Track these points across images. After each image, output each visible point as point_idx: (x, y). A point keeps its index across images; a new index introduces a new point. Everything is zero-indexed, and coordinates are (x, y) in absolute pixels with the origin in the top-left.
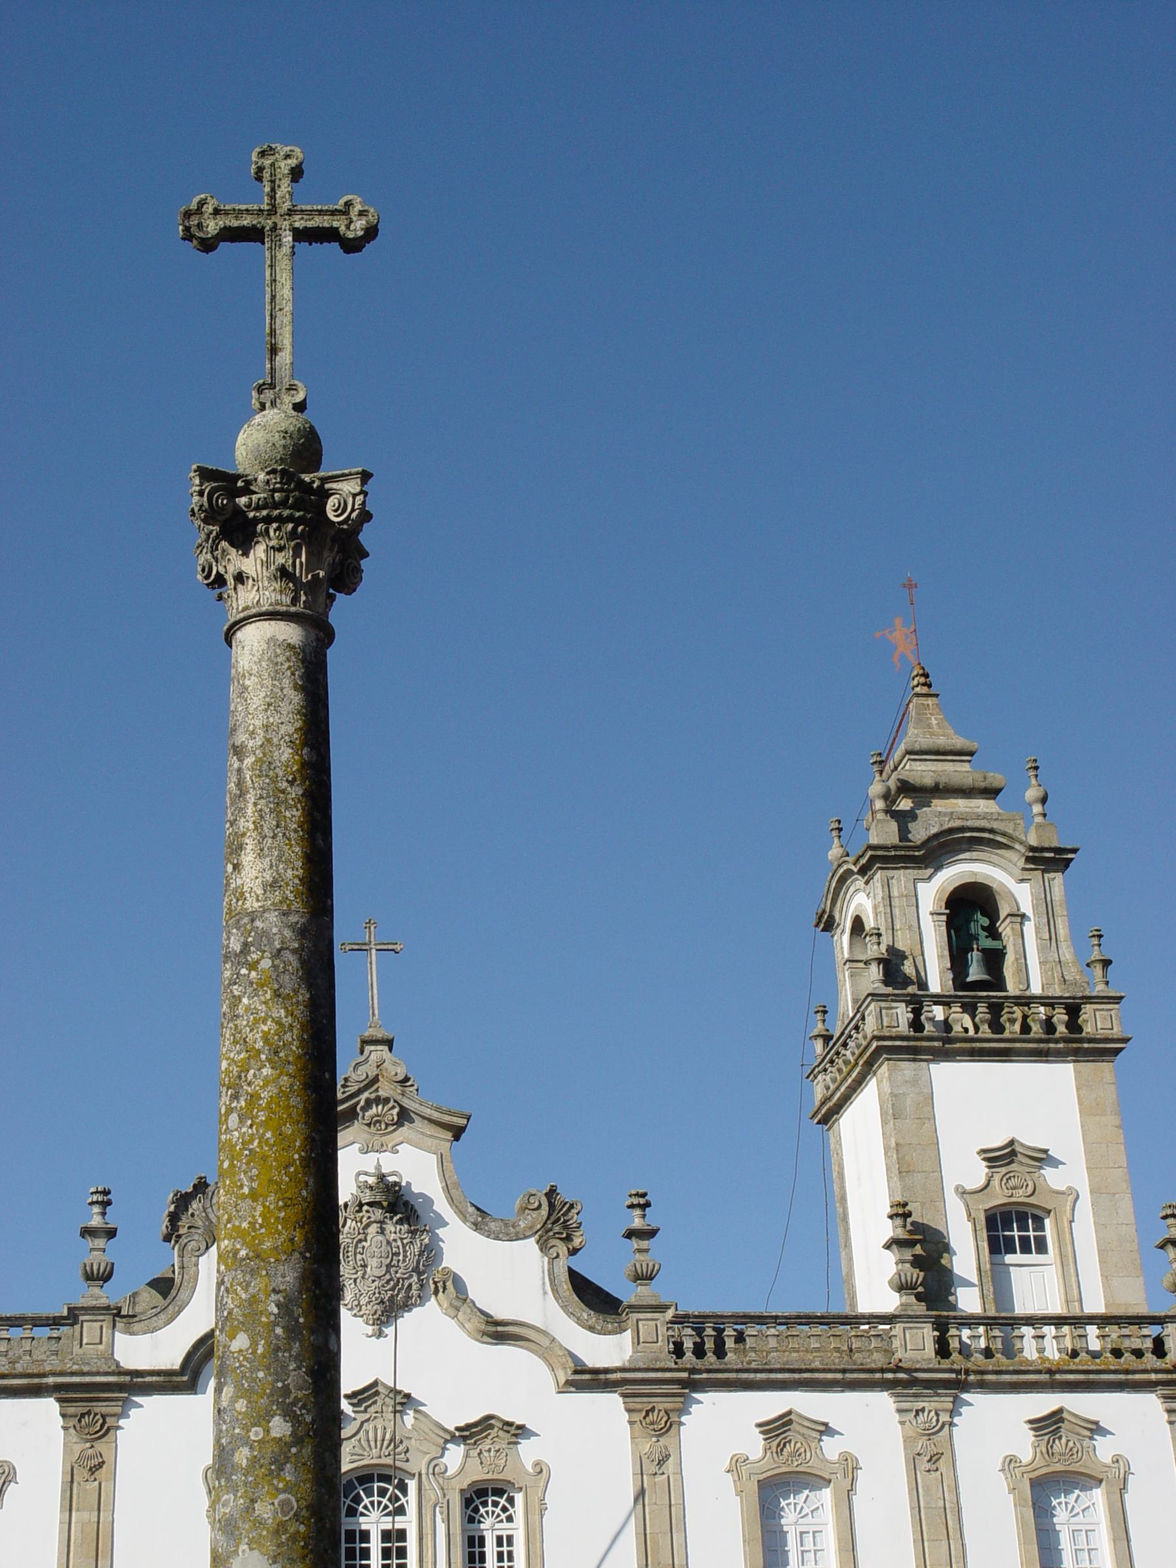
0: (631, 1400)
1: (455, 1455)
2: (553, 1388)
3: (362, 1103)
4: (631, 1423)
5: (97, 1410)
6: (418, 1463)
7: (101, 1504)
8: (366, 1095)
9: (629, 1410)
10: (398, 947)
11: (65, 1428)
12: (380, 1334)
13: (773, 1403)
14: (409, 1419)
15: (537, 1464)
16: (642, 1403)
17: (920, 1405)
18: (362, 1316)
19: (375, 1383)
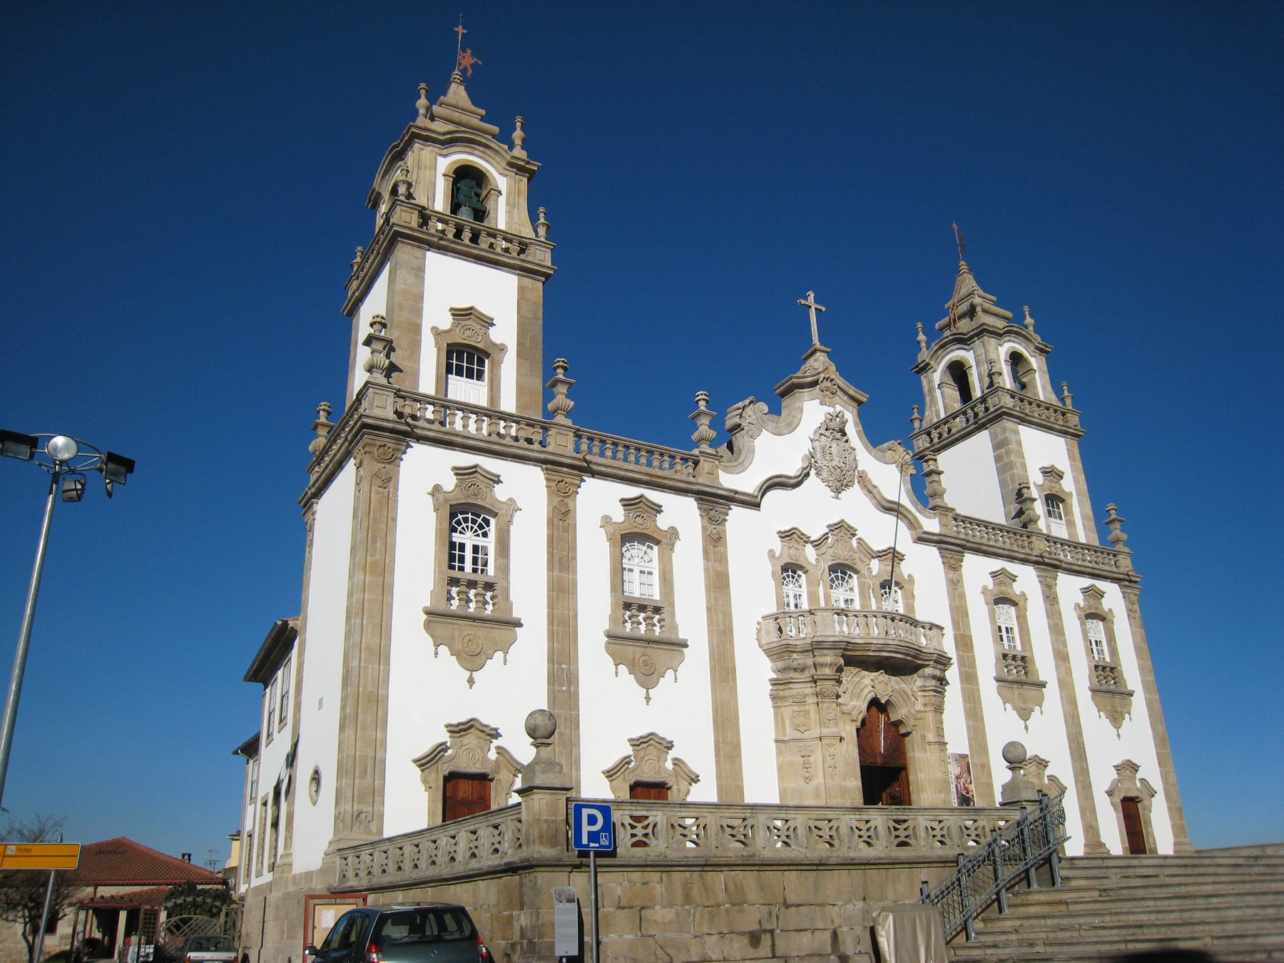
0: (943, 551)
1: (875, 565)
2: (911, 541)
3: (821, 379)
4: (943, 563)
5: (716, 509)
6: (859, 566)
7: (722, 559)
8: (822, 376)
9: (942, 557)
10: (824, 309)
11: (701, 516)
12: (837, 498)
13: (997, 564)
14: (854, 542)
15: (910, 576)
16: (946, 553)
17: (1047, 574)
18: (830, 487)
19: (842, 521)
